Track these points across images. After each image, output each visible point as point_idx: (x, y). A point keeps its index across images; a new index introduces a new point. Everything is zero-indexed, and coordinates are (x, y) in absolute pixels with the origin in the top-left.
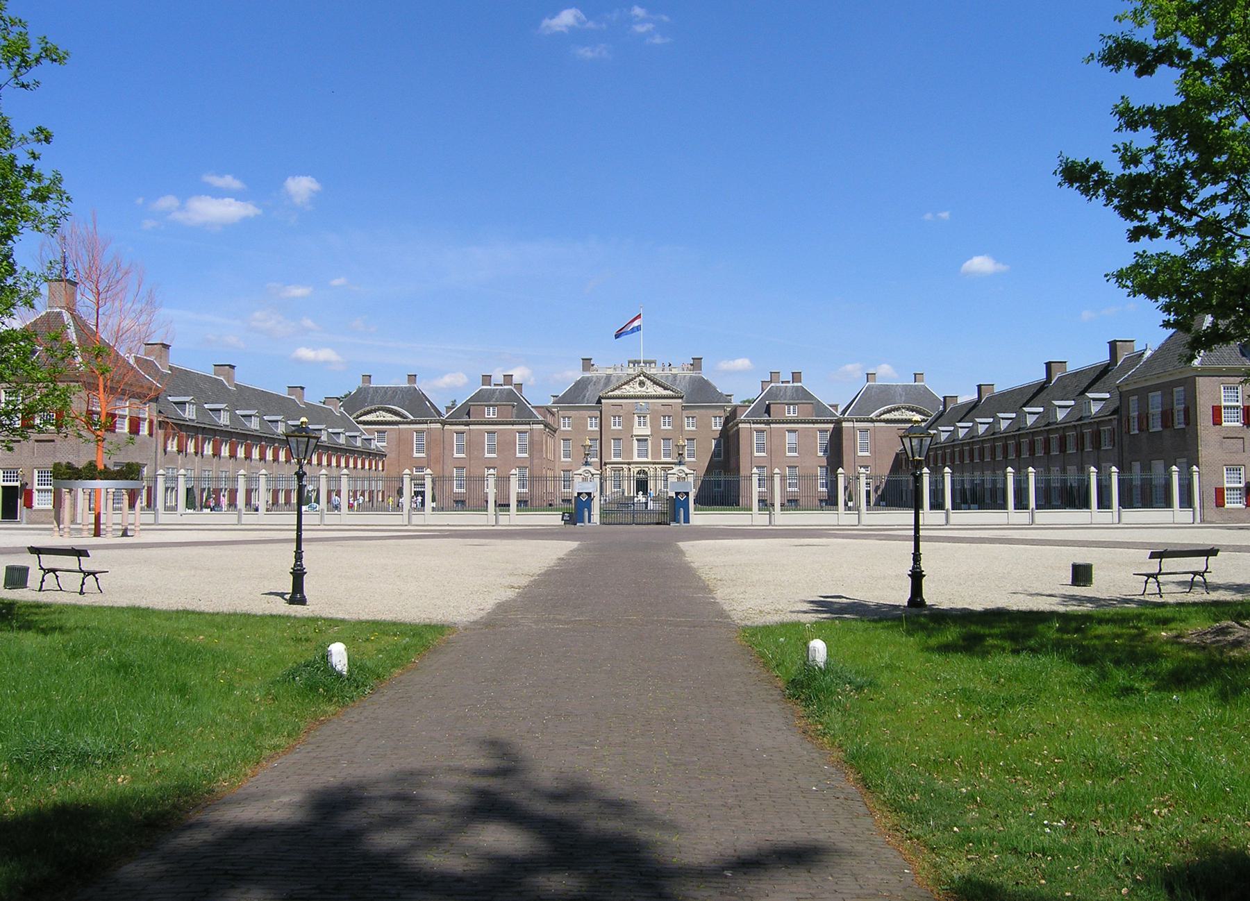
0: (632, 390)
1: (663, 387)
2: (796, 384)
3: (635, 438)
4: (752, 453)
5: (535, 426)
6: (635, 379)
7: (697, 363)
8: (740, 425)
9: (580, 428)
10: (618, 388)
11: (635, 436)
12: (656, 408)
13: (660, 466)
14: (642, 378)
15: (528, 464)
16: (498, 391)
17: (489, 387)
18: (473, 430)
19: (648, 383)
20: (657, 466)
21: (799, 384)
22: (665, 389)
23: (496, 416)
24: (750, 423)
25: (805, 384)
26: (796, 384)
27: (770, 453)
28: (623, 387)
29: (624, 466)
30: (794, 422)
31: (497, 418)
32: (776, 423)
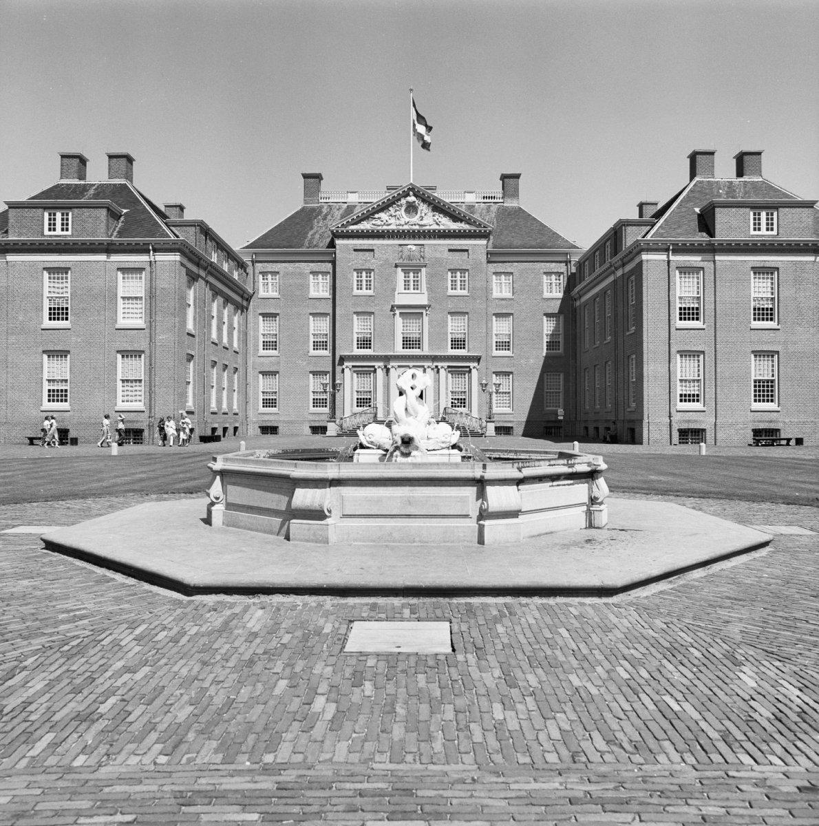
0: (393, 221)
3: (397, 312)
5: (160, 257)
6: (400, 200)
7: (509, 180)
9: (294, 293)
10: (367, 216)
11: (400, 307)
12: (438, 255)
13: (446, 364)
14: (412, 199)
15: (143, 345)
17: (76, 182)
18: (15, 263)
19: (423, 207)
20: (440, 364)
22: (455, 218)
24: (667, 250)
28: (376, 216)
29: (377, 364)
31: (72, 235)
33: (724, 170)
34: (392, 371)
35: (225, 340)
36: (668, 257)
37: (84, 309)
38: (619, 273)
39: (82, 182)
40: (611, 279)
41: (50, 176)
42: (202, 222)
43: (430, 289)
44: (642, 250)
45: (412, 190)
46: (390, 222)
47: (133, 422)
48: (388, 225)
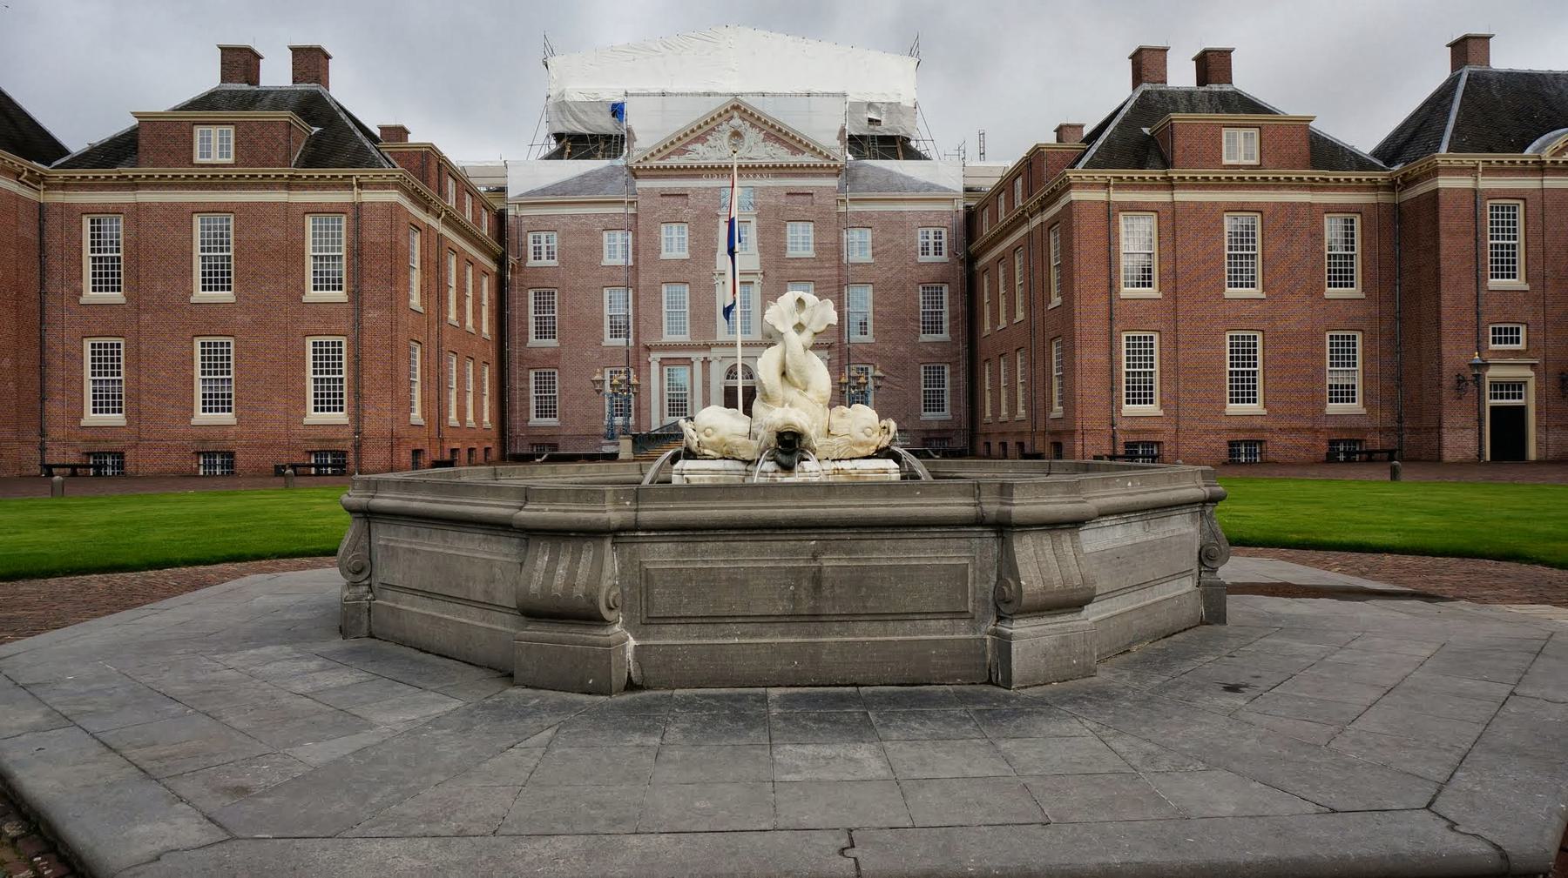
1: (790, 147)
2: (1215, 88)
4: (1112, 286)
5: (368, 196)
8: (1075, 195)
12: (773, 201)
14: (736, 122)
16: (271, 96)
17: (245, 87)
19: (752, 135)
21: (1226, 88)
23: (231, 160)
24: (1107, 186)
25: (1244, 79)
26: (1215, 88)
27: (1173, 282)
28: (690, 148)
29: (693, 355)
30: (1253, 184)
31: (236, 165)
32: (1195, 184)
33: (1181, 75)
34: (714, 366)
35: (469, 323)
36: (1109, 193)
37: (254, 274)
38: (1036, 222)
39: (255, 88)
40: (1024, 230)
41: (207, 78)
42: (432, 148)
43: (763, 249)
44: (1069, 187)
45: (737, 108)
46: (707, 155)
47: (330, 440)
48: (706, 159)
